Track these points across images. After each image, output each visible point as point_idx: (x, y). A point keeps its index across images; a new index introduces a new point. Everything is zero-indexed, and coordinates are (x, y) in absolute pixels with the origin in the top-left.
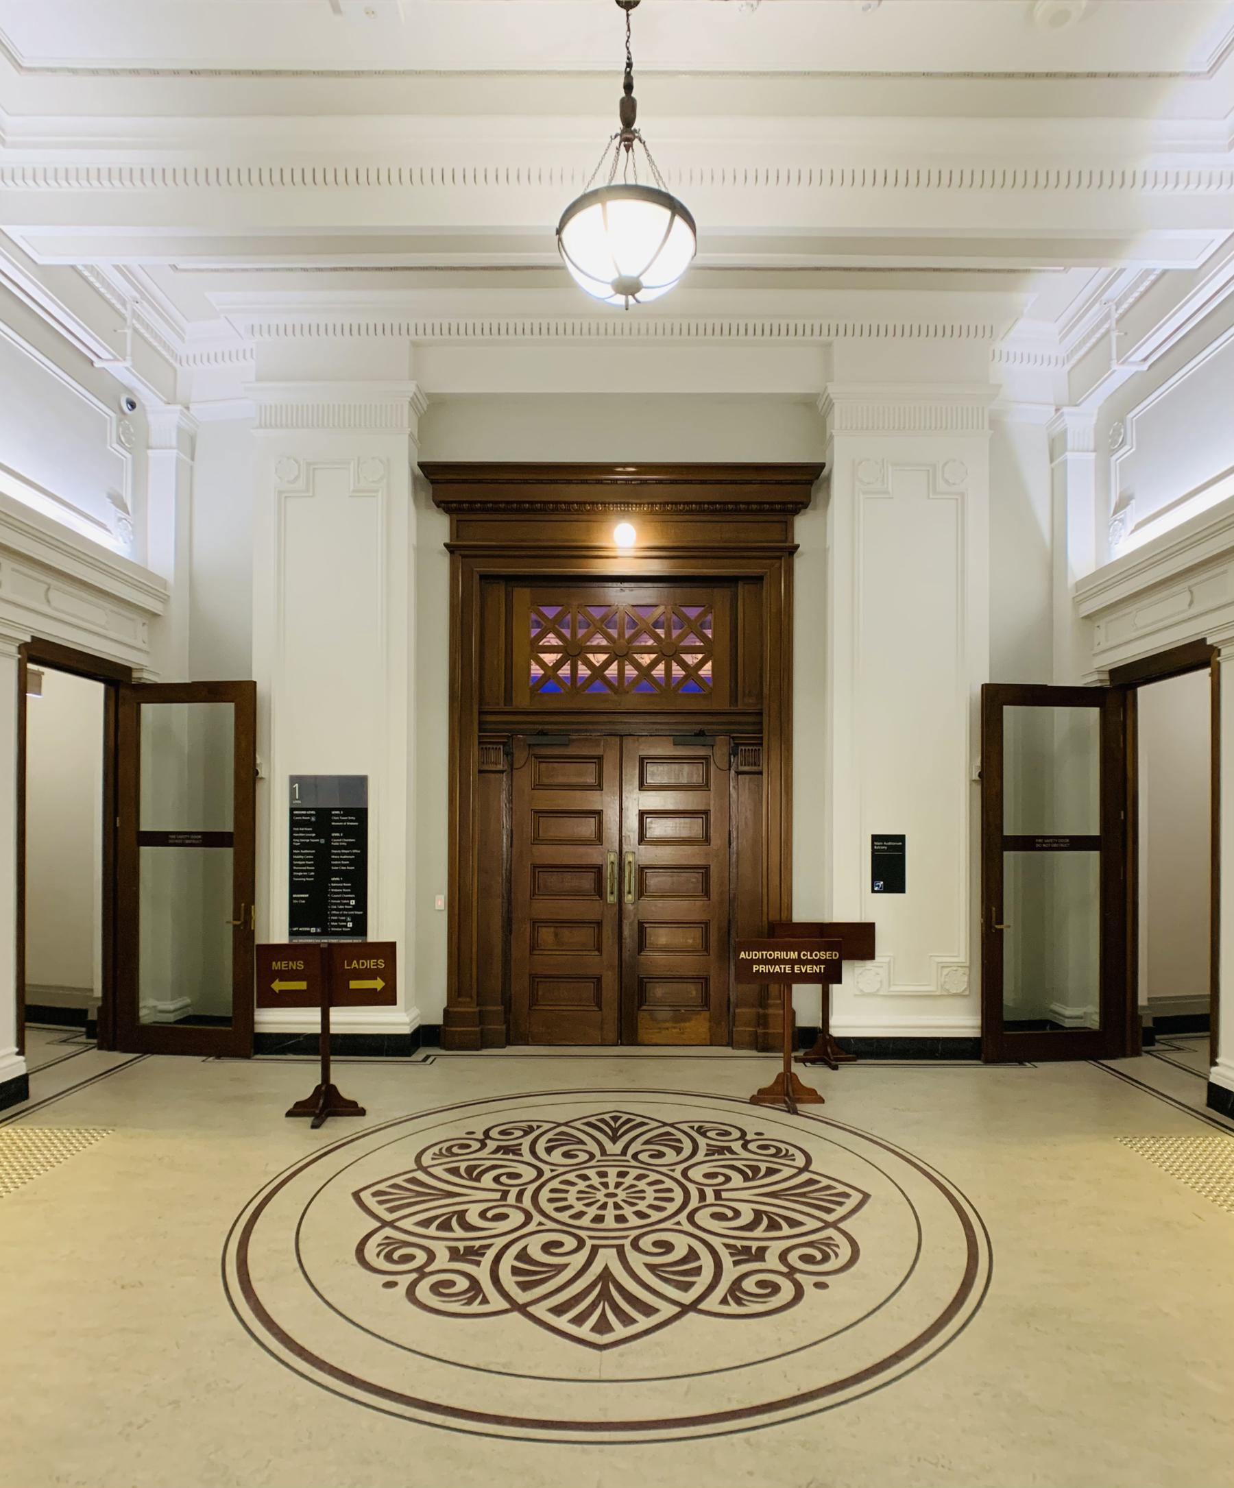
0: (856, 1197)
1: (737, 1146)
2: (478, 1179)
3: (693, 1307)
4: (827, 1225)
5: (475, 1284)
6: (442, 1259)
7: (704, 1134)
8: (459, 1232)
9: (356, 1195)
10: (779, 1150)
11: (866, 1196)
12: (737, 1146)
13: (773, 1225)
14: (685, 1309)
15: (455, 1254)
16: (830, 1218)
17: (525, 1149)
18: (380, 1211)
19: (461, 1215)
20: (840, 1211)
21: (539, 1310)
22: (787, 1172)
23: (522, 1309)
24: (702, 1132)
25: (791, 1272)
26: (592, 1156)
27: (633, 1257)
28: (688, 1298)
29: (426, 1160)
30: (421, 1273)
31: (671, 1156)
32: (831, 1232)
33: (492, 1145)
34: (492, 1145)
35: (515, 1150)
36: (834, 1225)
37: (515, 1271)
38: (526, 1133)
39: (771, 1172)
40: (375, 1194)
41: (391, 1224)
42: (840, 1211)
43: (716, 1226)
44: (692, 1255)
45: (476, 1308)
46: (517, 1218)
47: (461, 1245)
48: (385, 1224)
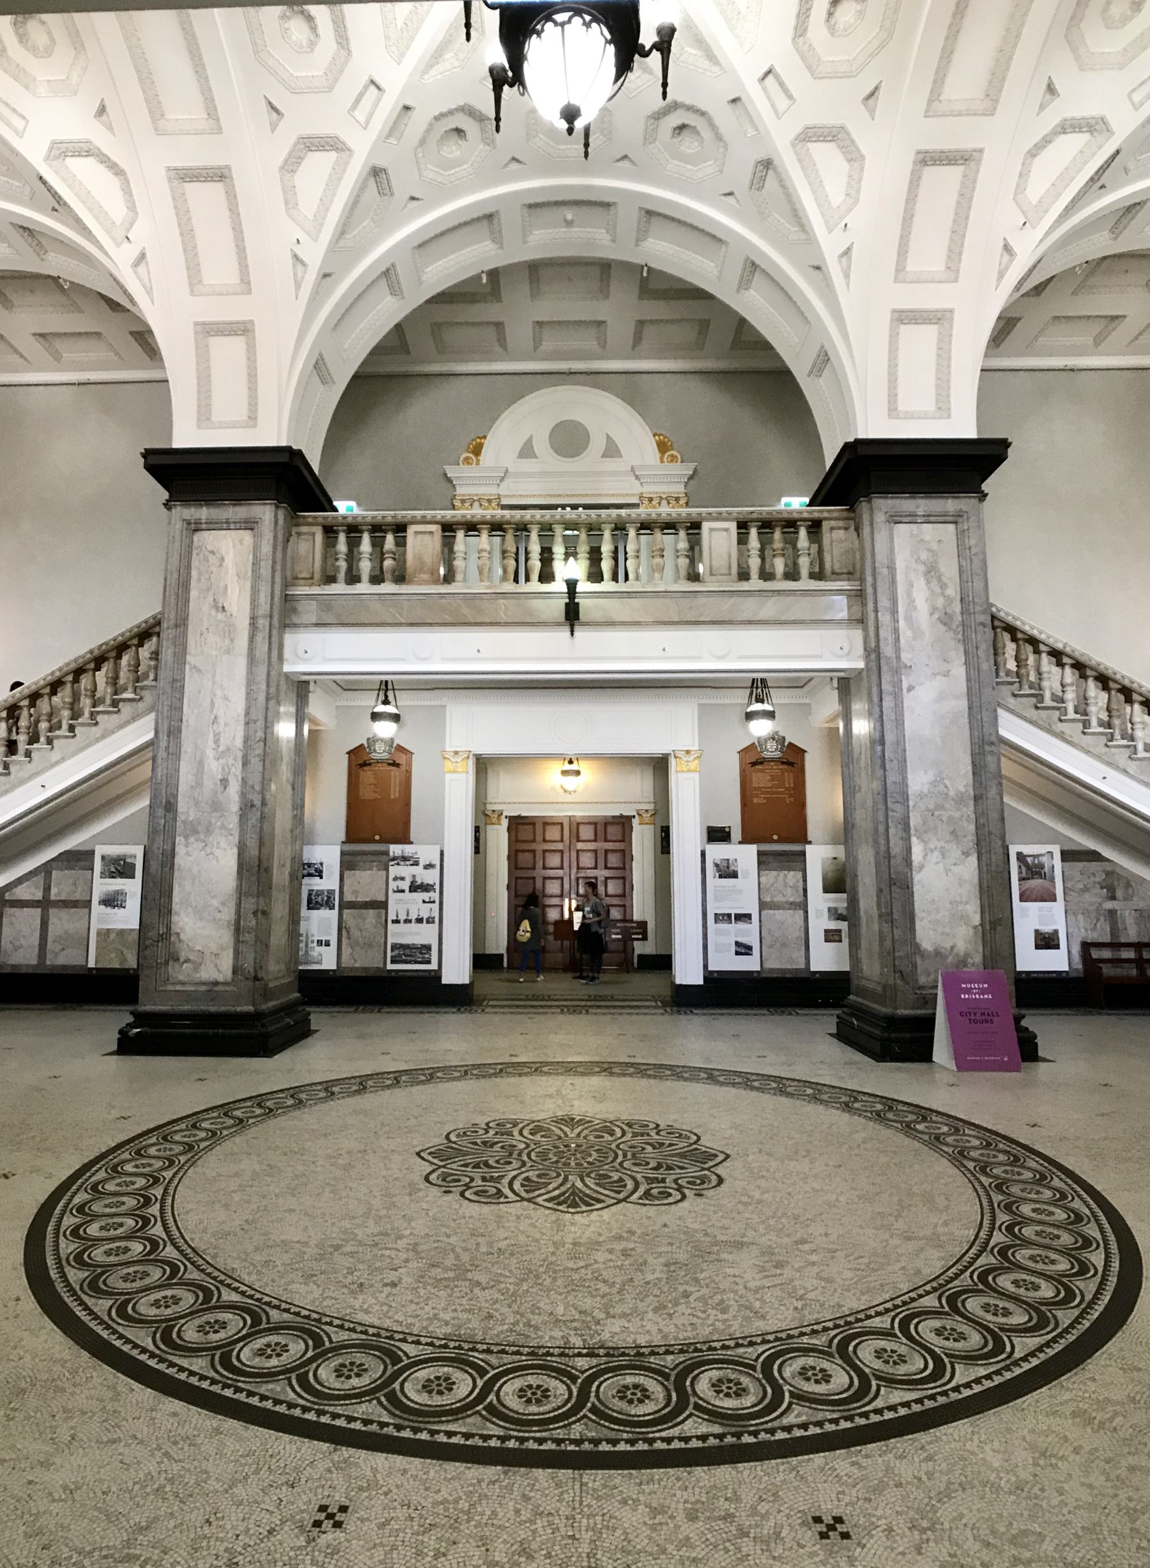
0: (721, 1157)
1: (653, 1133)
2: (492, 1146)
3: (624, 1200)
4: (703, 1169)
5: (499, 1191)
6: (478, 1182)
7: (630, 1127)
8: (486, 1170)
9: (418, 1154)
10: (681, 1135)
11: (728, 1156)
12: (653, 1133)
13: (669, 1168)
14: (619, 1201)
15: (484, 1179)
16: (706, 1166)
17: (516, 1133)
18: (435, 1161)
19: (487, 1165)
20: (711, 1163)
21: (540, 1200)
22: (681, 1145)
23: (529, 1200)
24: (630, 1125)
25: (680, 1189)
26: (560, 1138)
27: (587, 1180)
28: (621, 1196)
29: (453, 1138)
30: (468, 1187)
31: (607, 1137)
32: (706, 1172)
33: (492, 1132)
34: (492, 1132)
35: (510, 1134)
36: (708, 1169)
37: (522, 1185)
38: (514, 1126)
39: (671, 1145)
40: (430, 1154)
41: (444, 1167)
42: (711, 1163)
43: (636, 1169)
44: (621, 1180)
45: (502, 1200)
46: (516, 1164)
47: (487, 1175)
48: (440, 1167)
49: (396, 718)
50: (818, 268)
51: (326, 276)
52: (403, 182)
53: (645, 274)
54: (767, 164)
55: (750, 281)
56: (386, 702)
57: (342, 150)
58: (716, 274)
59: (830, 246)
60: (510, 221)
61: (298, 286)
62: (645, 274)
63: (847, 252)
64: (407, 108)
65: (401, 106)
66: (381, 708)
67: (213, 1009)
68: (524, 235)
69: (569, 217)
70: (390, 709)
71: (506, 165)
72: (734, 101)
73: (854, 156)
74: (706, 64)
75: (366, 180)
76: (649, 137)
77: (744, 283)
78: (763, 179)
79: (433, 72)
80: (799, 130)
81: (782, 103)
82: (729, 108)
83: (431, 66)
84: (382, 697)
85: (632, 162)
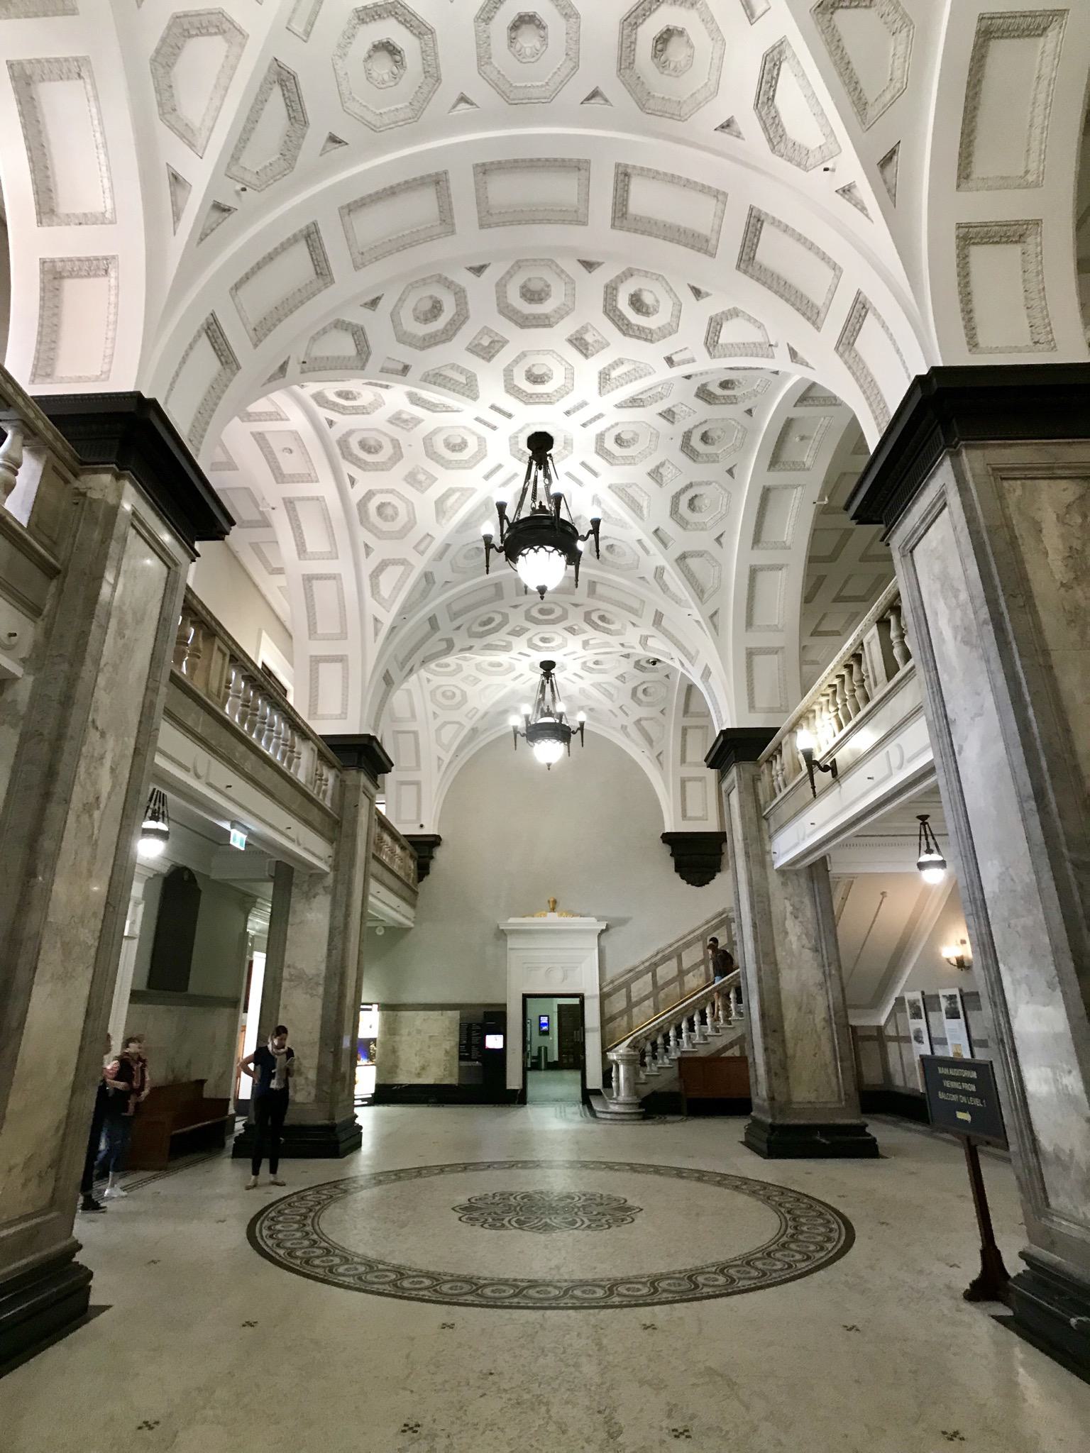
49: (942, 864)
52: (702, 541)
56: (929, 851)
66: (925, 858)
67: (802, 1122)
70: (935, 857)
79: (645, 511)
83: (642, 512)
84: (924, 848)
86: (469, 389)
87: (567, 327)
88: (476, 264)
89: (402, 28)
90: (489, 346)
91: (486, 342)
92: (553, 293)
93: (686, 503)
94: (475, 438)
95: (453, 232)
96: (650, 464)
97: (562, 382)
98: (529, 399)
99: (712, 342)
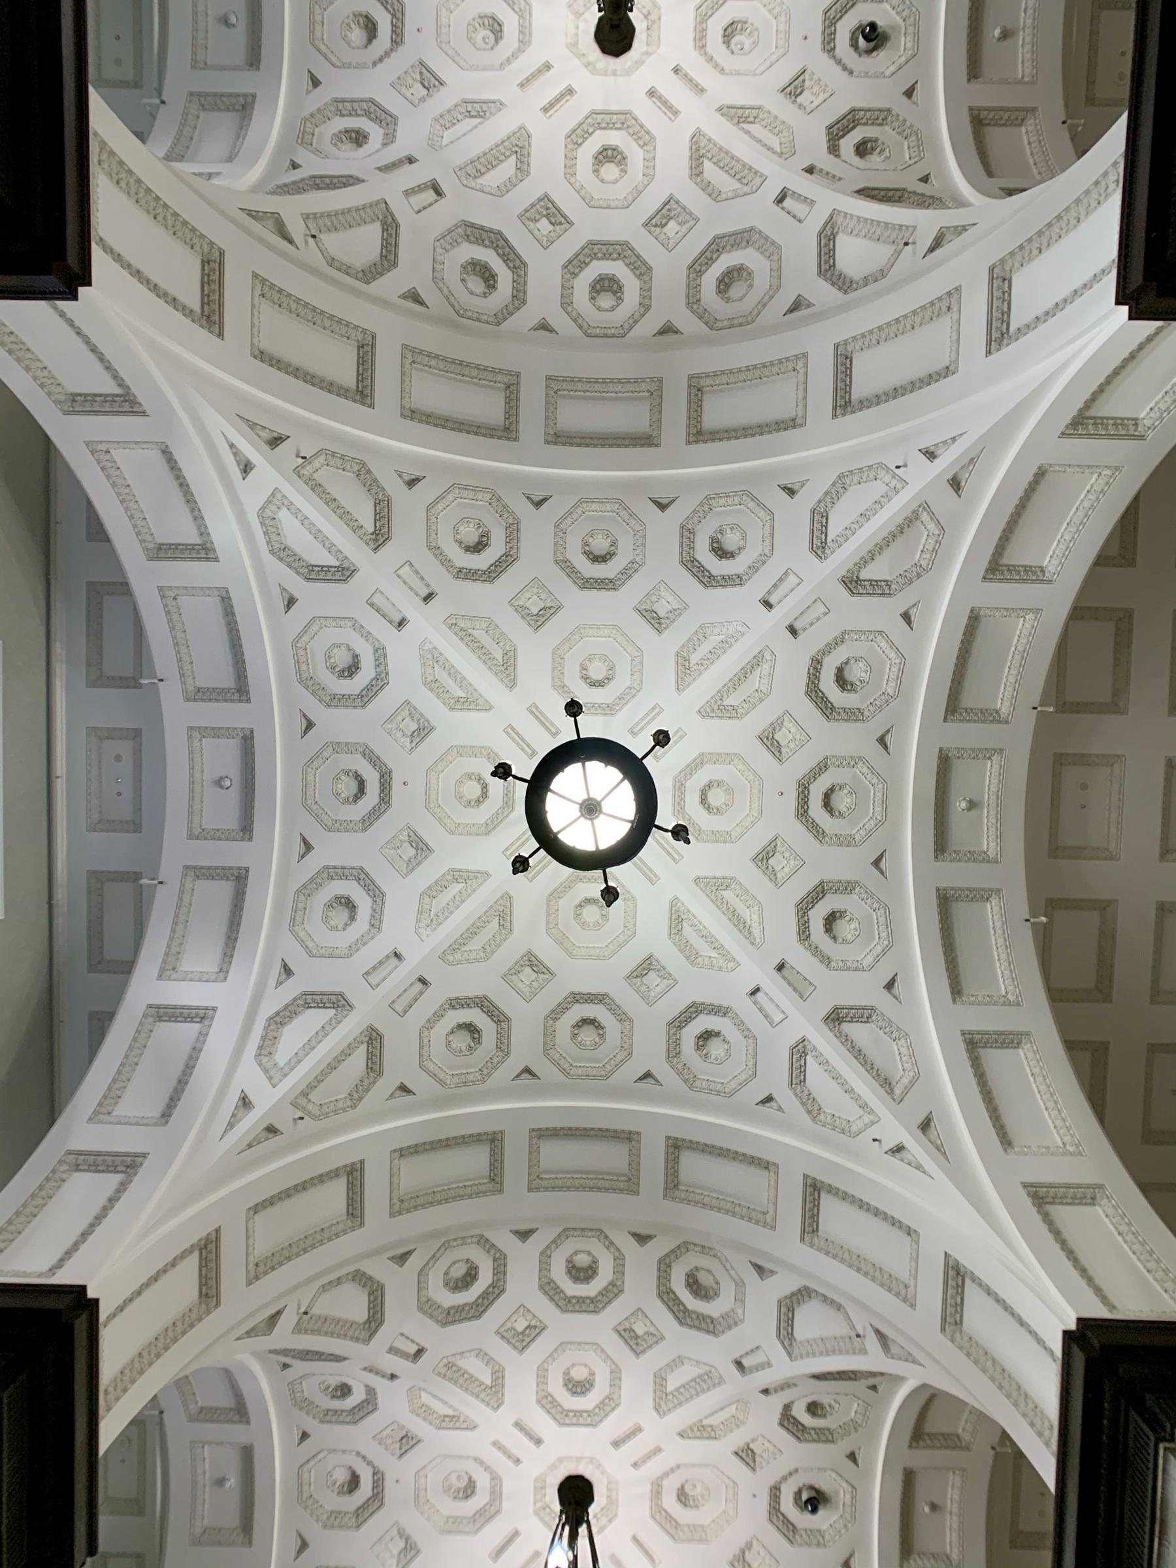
50: (955, 484)
51: (925, 1126)
52: (860, 990)
53: (1052, 709)
54: (853, 583)
55: (1027, 569)
57: (804, 1047)
58: (1030, 616)
59: (922, 477)
60: (954, 875)
61: (919, 1167)
62: (1052, 709)
63: (930, 455)
64: (781, 967)
65: (775, 973)
68: (986, 860)
69: (964, 805)
71: (882, 873)
72: (793, 631)
73: (839, 487)
74: (766, 667)
75: (839, 1035)
76: (854, 715)
77: (1033, 575)
78: (874, 583)
79: (756, 932)
80: (812, 557)
81: (792, 580)
82: (802, 636)
85: (888, 731)
86: (494, 1393)
87: (616, 1312)
88: (523, 1227)
89: (485, 1016)
90: (523, 1333)
91: (520, 1326)
92: (600, 1271)
93: (820, 914)
94: (487, 1476)
95: (501, 1191)
96: (757, 841)
97: (610, 1277)
98: (565, 1417)
99: (820, 546)
